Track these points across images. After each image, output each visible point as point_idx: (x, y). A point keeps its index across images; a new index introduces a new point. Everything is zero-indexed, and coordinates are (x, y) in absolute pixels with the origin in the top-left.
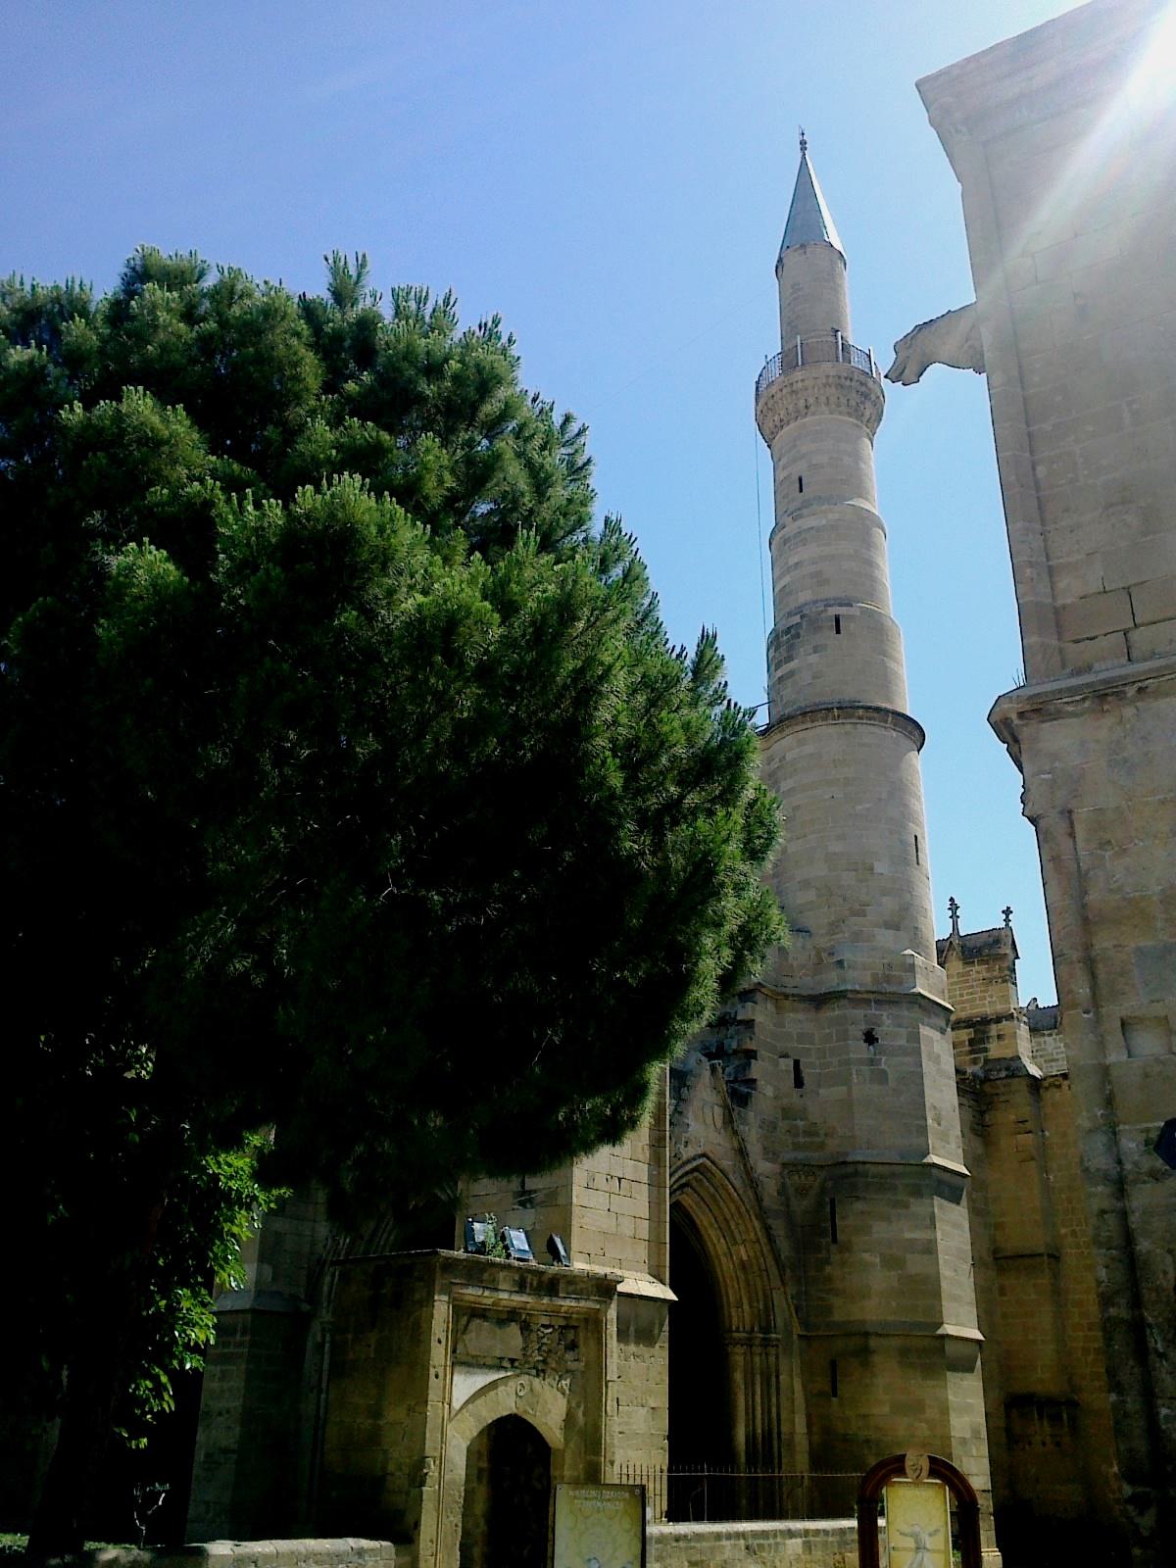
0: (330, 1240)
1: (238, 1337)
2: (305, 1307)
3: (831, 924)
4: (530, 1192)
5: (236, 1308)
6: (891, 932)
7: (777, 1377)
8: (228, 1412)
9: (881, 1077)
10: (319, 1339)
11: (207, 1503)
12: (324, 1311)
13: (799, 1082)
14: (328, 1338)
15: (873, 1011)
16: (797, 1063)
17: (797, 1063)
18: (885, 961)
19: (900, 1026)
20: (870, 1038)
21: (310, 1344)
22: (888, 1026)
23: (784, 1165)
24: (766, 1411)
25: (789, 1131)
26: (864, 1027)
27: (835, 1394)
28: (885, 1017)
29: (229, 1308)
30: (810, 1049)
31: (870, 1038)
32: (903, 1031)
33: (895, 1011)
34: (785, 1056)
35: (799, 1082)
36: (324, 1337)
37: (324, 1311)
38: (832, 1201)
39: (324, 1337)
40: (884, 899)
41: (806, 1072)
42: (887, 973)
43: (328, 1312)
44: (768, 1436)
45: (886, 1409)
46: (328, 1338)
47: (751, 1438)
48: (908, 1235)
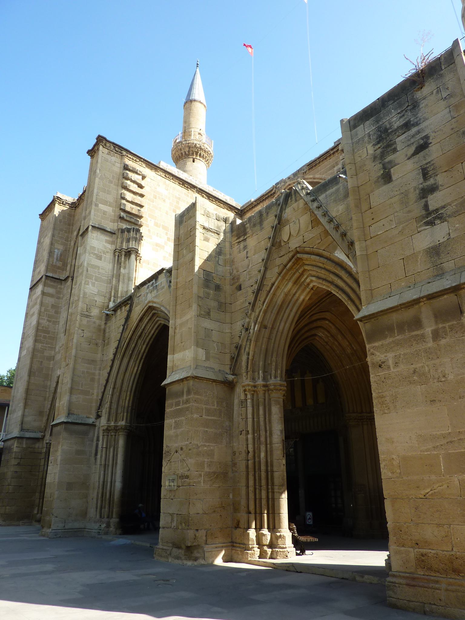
0: (243, 332)
1: (185, 397)
2: (231, 377)
4: (437, 210)
5: (182, 377)
8: (182, 449)
10: (242, 397)
11: (172, 515)
12: (244, 378)
14: (249, 396)
21: (236, 401)
29: (177, 379)
36: (246, 395)
37: (244, 378)
39: (246, 395)
43: (247, 379)
46: (249, 396)
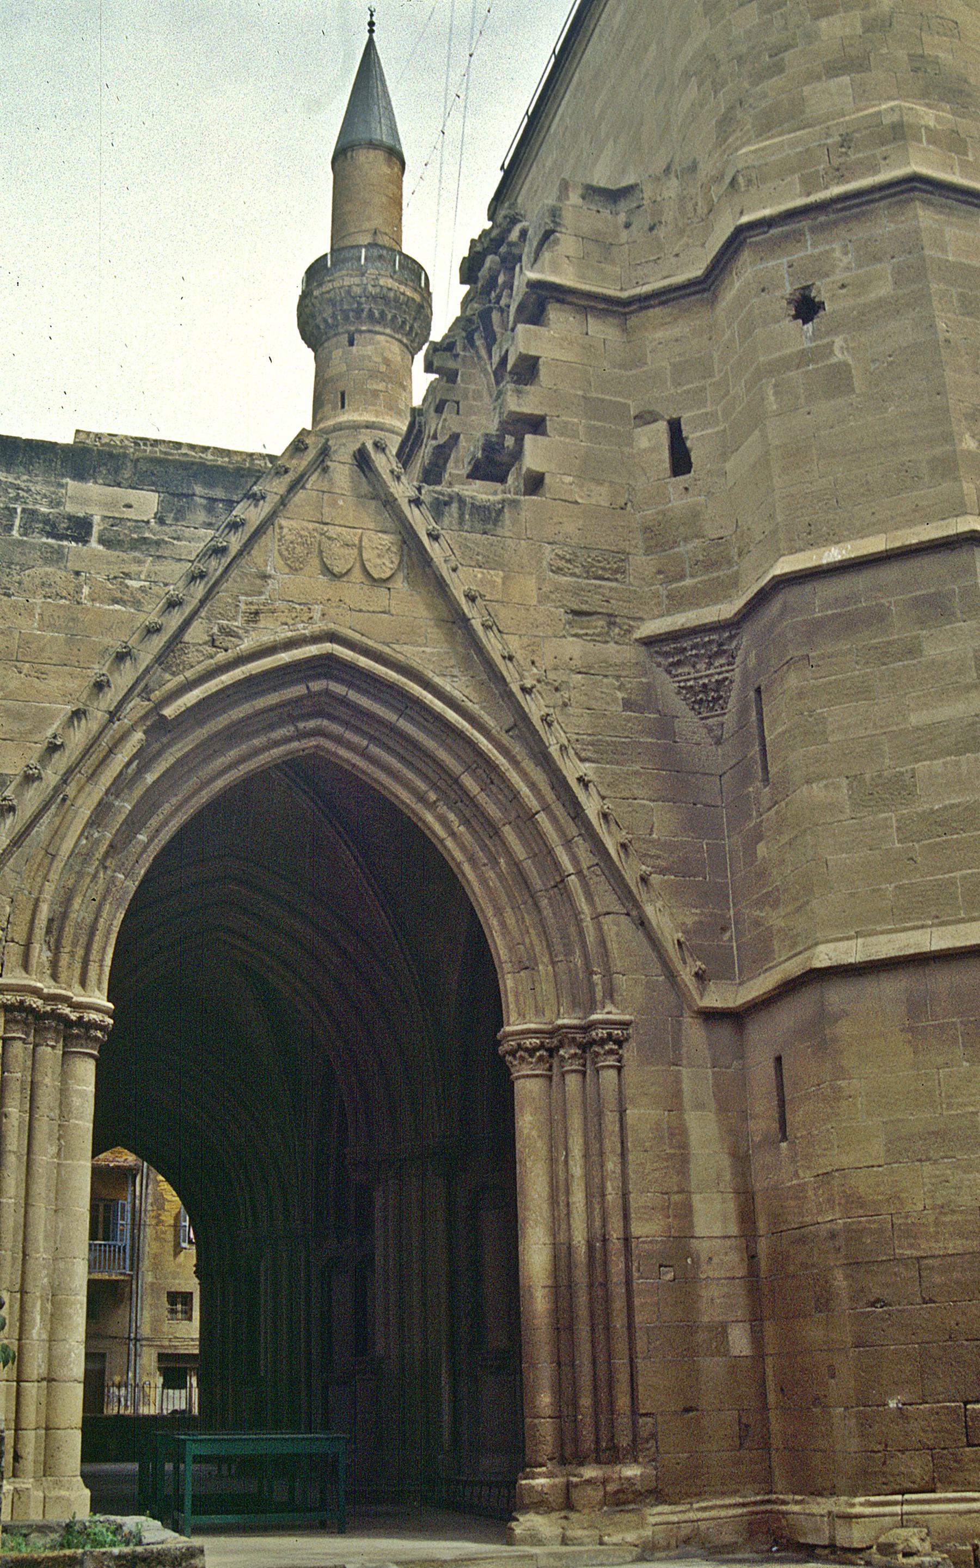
3: (720, 123)
6: (846, 79)
7: (622, 1112)
9: (839, 380)
13: (681, 461)
15: (808, 249)
16: (675, 428)
17: (675, 428)
18: (829, 141)
19: (876, 259)
20: (806, 308)
22: (848, 269)
23: (649, 642)
24: (595, 1193)
25: (660, 572)
26: (788, 289)
27: (784, 1138)
28: (837, 254)
30: (703, 389)
31: (806, 308)
32: (886, 267)
33: (860, 231)
34: (646, 418)
35: (681, 461)
38: (758, 691)
40: (823, 23)
41: (692, 437)
42: (836, 162)
44: (598, 1246)
45: (877, 1150)
47: (561, 1257)
48: (915, 719)
